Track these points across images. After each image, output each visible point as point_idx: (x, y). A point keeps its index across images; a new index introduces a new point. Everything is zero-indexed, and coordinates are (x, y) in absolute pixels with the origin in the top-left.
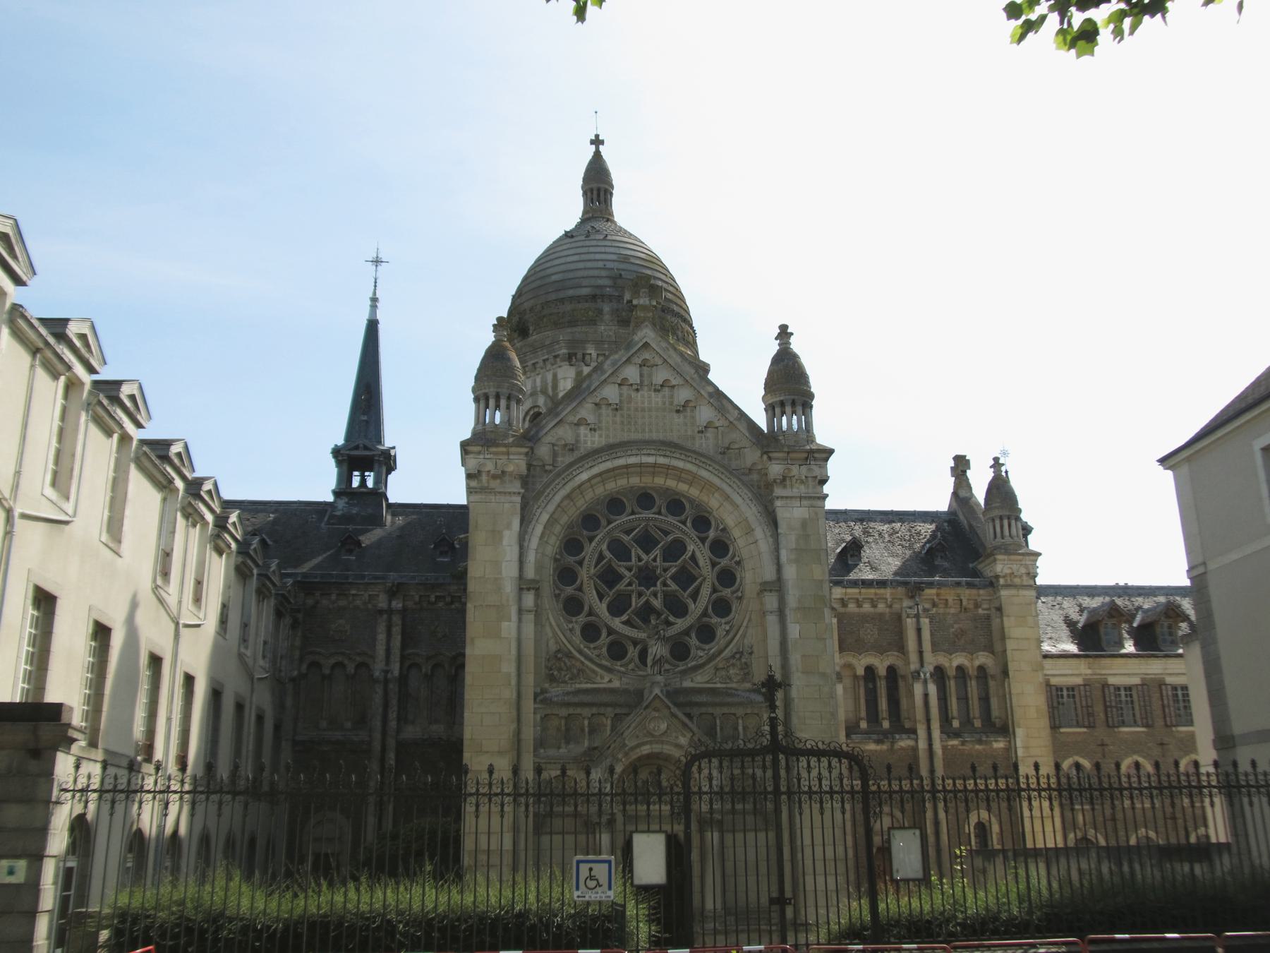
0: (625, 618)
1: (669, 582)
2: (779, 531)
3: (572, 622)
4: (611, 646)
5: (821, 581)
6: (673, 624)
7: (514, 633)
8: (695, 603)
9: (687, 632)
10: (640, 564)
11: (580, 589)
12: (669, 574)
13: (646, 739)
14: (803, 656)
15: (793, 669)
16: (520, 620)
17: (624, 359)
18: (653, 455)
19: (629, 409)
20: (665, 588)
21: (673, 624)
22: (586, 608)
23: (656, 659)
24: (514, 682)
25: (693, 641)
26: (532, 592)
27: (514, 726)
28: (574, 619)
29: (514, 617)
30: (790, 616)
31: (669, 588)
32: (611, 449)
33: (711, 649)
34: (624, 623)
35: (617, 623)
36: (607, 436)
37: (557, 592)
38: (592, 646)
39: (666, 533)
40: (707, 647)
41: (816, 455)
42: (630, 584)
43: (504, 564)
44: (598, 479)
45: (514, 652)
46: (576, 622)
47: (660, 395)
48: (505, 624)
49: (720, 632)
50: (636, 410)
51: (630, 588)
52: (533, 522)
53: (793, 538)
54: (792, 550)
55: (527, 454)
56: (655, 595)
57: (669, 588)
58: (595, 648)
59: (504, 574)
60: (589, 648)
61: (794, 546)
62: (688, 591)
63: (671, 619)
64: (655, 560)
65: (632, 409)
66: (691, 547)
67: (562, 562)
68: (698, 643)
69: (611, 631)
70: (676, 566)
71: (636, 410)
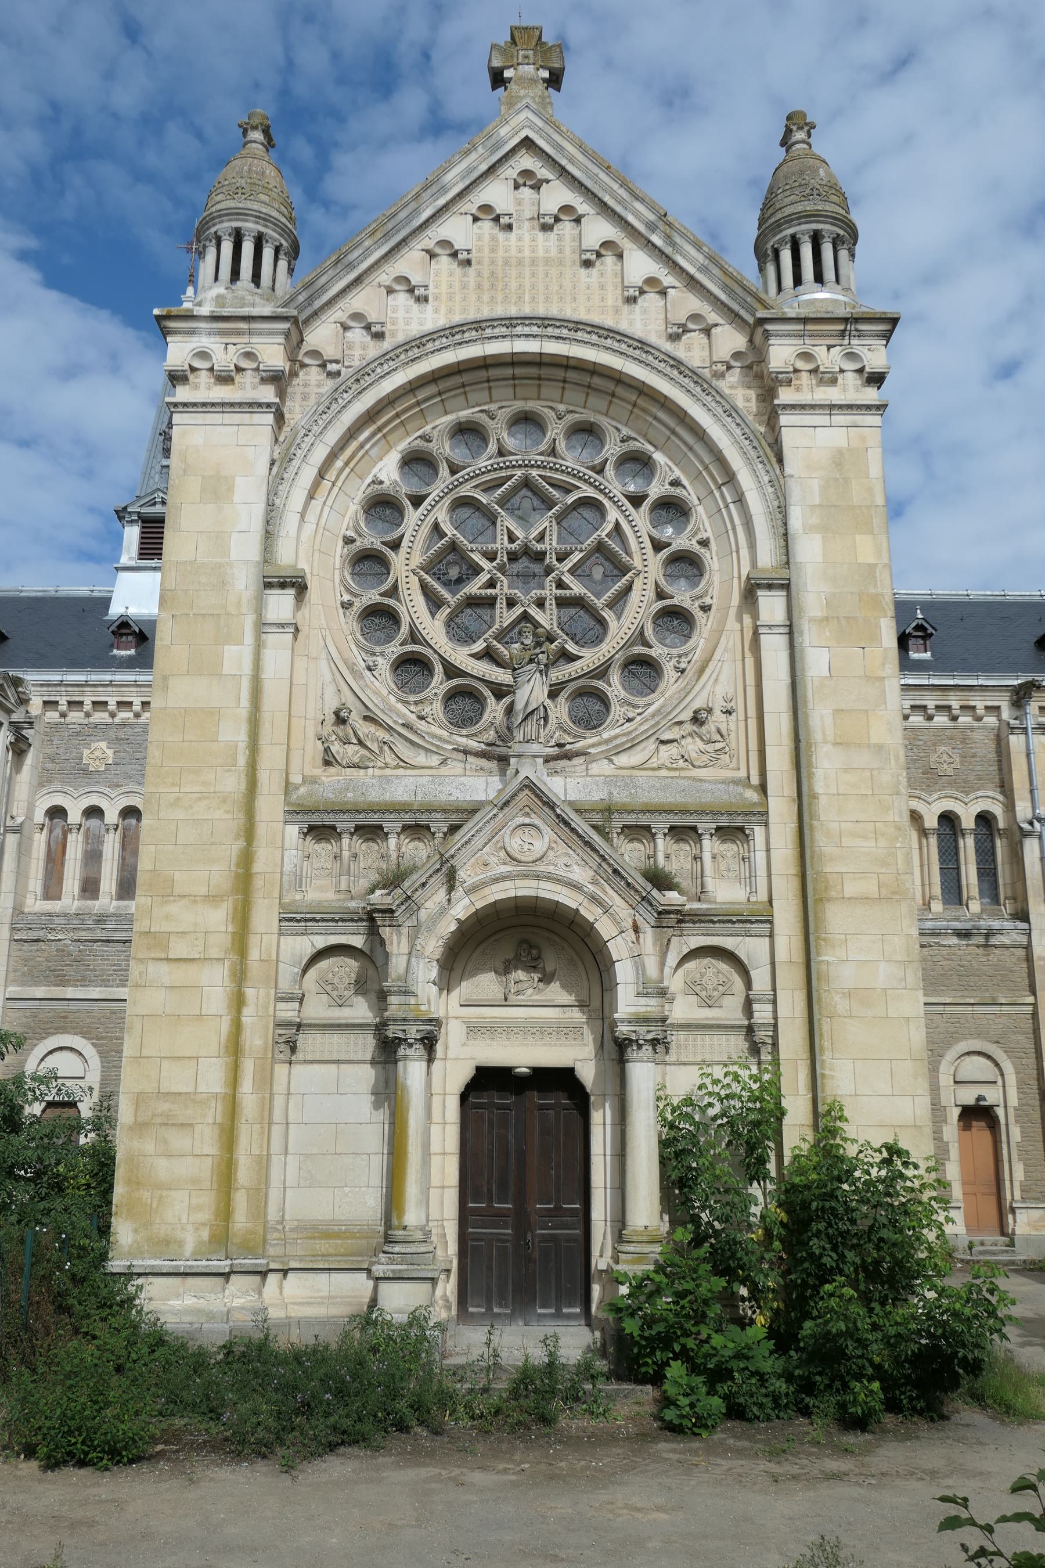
0: (479, 646)
1: (567, 579)
2: (788, 470)
3: (374, 654)
4: (451, 696)
5: (872, 567)
6: (576, 658)
7: (247, 669)
8: (619, 618)
9: (601, 672)
10: (513, 546)
11: (393, 592)
12: (569, 564)
13: (503, 869)
14: (837, 711)
15: (817, 736)
16: (259, 647)
17: (484, 167)
18: (535, 336)
19: (493, 262)
20: (559, 592)
21: (576, 658)
22: (404, 629)
23: (530, 709)
24: (242, 761)
25: (615, 687)
26: (292, 592)
27: (241, 843)
28: (378, 649)
29: (249, 638)
30: (809, 636)
31: (568, 592)
32: (454, 332)
33: (650, 705)
34: (477, 656)
35: (461, 656)
36: (450, 311)
37: (346, 597)
38: (412, 698)
39: (567, 489)
40: (641, 701)
41: (862, 327)
42: (491, 584)
43: (234, 536)
44: (432, 389)
45: (245, 702)
46: (382, 654)
47: (552, 236)
48: (230, 651)
49: (668, 669)
50: (506, 262)
51: (490, 591)
52: (296, 463)
53: (815, 484)
54: (813, 507)
55: (287, 335)
56: (540, 603)
57: (568, 592)
58: (416, 703)
59: (234, 555)
60: (406, 703)
61: (817, 502)
62: (605, 597)
63: (571, 648)
64: (541, 538)
65: (500, 262)
66: (613, 515)
67: (358, 543)
68: (623, 694)
69: (451, 671)
70: (581, 551)
71: (506, 262)
